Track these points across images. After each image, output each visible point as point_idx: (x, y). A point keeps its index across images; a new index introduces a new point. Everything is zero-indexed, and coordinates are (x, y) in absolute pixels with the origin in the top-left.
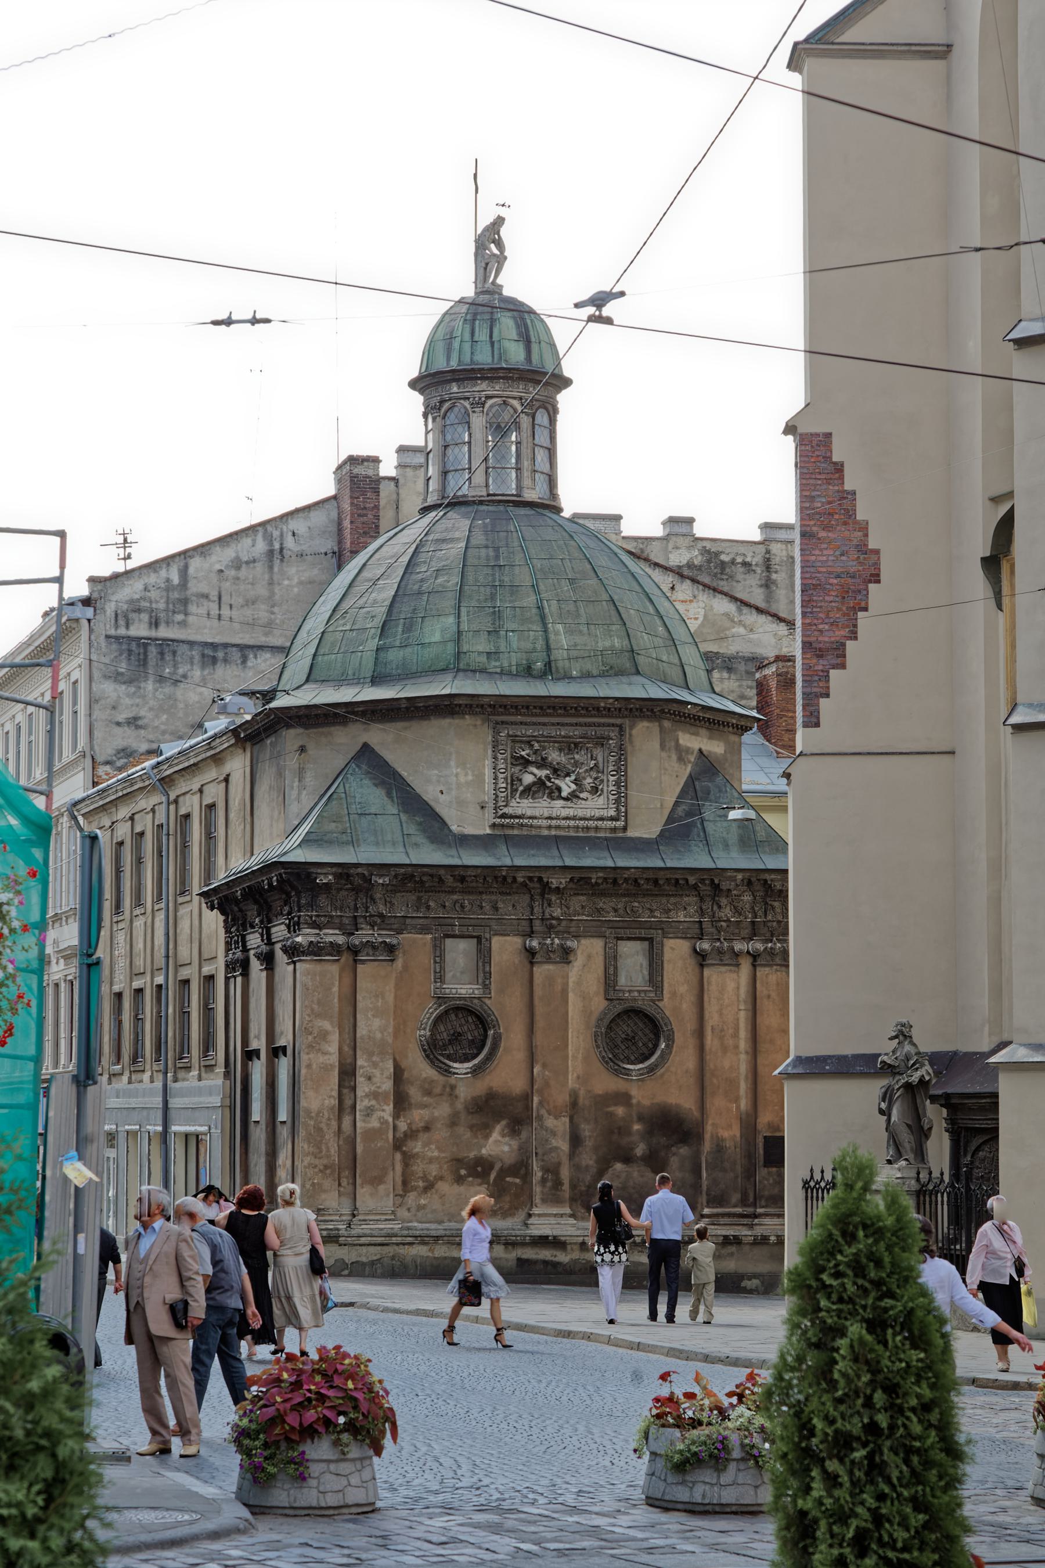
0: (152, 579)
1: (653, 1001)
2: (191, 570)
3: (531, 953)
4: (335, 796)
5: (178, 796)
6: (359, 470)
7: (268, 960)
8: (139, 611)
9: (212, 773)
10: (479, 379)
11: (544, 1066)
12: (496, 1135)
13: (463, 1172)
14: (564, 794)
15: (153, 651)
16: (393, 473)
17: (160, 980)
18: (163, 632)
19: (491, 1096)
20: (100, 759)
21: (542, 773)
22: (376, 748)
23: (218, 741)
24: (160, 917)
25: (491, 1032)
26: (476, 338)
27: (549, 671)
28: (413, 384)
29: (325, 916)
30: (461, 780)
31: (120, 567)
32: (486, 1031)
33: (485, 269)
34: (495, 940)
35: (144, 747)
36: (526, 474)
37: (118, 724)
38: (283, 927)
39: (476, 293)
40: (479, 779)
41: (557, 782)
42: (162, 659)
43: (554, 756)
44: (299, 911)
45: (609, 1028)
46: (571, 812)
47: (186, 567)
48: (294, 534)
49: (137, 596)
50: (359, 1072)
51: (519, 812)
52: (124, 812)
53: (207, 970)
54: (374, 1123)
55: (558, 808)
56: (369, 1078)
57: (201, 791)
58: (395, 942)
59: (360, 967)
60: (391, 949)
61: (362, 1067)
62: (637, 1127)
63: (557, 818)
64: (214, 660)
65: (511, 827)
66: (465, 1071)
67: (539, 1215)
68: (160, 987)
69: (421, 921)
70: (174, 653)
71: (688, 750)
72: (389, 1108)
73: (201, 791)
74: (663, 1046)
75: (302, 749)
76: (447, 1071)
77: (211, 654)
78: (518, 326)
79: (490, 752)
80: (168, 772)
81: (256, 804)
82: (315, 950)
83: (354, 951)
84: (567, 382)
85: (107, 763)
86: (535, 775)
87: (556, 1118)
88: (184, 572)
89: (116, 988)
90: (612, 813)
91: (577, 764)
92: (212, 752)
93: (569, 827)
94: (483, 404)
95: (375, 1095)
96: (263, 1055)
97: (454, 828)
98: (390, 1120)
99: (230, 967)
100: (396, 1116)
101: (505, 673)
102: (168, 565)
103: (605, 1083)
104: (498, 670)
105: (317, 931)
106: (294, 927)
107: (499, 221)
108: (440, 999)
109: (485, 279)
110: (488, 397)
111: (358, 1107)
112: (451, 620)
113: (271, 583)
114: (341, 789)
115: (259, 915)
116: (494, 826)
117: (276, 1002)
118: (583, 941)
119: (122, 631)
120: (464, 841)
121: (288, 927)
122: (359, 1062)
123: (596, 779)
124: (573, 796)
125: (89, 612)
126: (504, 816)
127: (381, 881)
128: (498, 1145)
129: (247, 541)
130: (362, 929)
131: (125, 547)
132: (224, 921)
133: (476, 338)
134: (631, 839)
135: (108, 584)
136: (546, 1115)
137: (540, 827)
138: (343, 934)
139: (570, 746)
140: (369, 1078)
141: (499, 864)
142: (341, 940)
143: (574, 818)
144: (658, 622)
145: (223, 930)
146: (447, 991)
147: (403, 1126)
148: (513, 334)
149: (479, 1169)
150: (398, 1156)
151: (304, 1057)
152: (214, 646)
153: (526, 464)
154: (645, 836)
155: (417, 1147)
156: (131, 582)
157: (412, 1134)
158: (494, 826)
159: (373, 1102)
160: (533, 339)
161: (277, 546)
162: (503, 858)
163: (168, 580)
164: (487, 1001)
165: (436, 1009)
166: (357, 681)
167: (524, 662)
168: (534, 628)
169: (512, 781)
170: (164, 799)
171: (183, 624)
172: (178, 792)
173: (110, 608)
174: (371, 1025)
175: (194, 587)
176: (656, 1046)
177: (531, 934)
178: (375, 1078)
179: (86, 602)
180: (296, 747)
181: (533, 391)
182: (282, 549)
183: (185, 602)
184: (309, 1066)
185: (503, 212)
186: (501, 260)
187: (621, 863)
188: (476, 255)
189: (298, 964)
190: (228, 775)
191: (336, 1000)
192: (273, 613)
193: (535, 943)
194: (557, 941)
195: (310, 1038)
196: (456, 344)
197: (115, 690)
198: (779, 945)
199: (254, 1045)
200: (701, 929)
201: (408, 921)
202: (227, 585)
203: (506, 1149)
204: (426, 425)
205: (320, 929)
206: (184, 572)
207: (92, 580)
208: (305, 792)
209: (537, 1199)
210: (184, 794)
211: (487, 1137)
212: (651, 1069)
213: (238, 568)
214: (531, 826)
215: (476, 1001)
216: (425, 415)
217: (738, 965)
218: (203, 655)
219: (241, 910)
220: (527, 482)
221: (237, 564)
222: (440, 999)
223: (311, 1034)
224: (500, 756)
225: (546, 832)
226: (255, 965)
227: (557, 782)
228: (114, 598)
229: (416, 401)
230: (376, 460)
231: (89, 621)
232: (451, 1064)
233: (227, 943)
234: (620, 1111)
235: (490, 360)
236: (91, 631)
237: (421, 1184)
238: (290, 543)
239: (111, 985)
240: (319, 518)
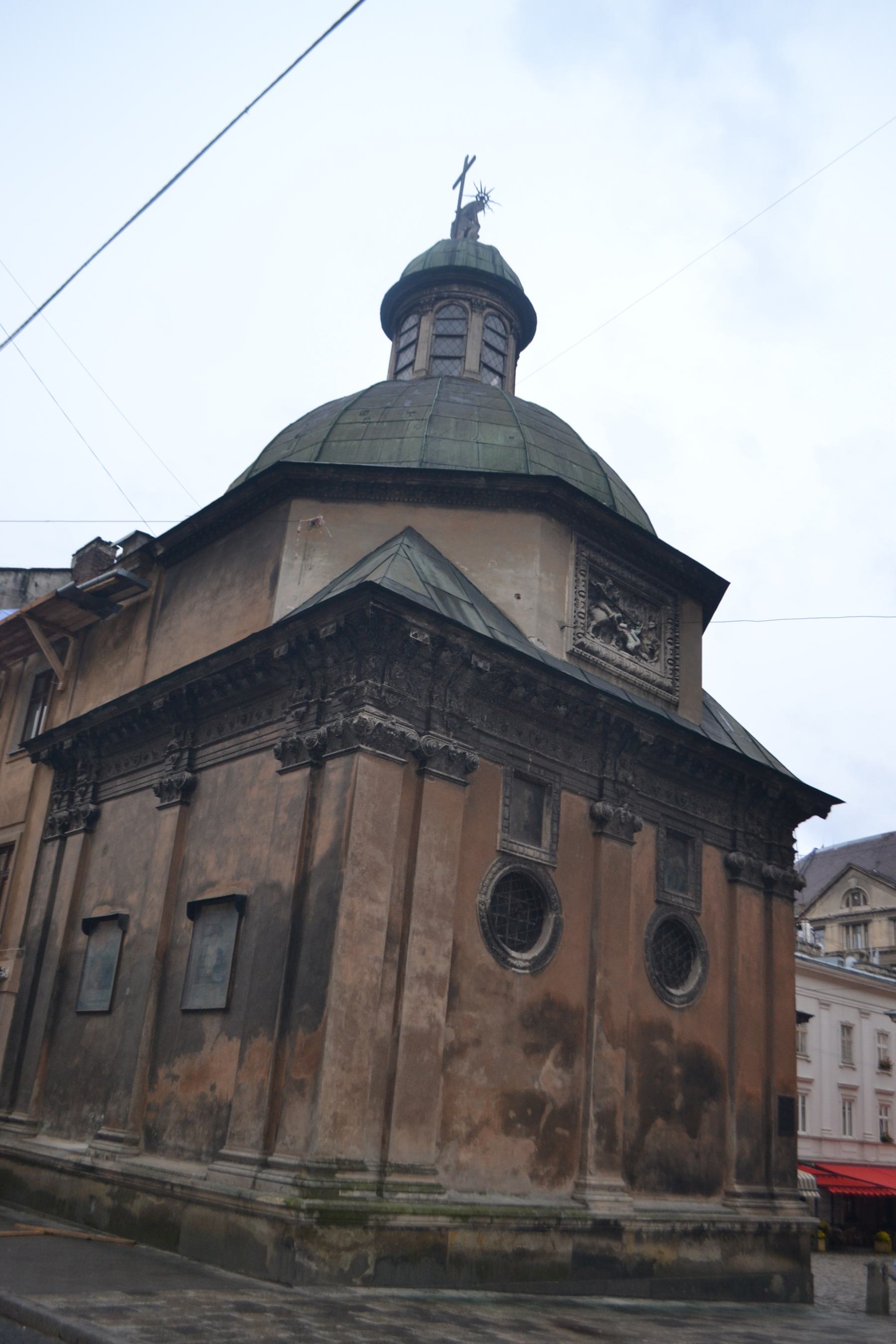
1: (692, 913)
3: (599, 821)
11: (606, 974)
12: (549, 1064)
13: (512, 1114)
19: (549, 1003)
29: (398, 695)
40: (561, 592)
44: (358, 680)
45: (657, 937)
54: (424, 1024)
59: (428, 783)
61: (417, 933)
62: (677, 1070)
63: (625, 669)
66: (522, 964)
67: (595, 1188)
69: (495, 744)
72: (442, 1003)
74: (700, 971)
76: (503, 961)
79: (571, 568)
86: (607, 613)
87: (614, 1048)
90: (668, 683)
94: (483, 308)
97: (533, 640)
98: (442, 1020)
100: (447, 1017)
103: (653, 1008)
108: (506, 856)
115: (177, 735)
116: (571, 654)
122: (414, 925)
126: (581, 646)
127: (481, 665)
128: (549, 1078)
130: (435, 729)
136: (604, 1041)
137: (610, 673)
139: (635, 598)
140: (423, 952)
143: (638, 675)
146: (515, 847)
149: (523, 1111)
151: (345, 902)
155: (462, 1067)
158: (571, 654)
159: (425, 991)
164: (550, 871)
165: (500, 869)
174: (434, 872)
177: (600, 797)
184: (350, 916)
191: (395, 822)
195: (357, 870)
201: (482, 738)
203: (559, 1084)
208: (309, 574)
209: (591, 1165)
211: (542, 1063)
212: (690, 997)
215: (540, 870)
222: (506, 856)
223: (358, 864)
224: (581, 578)
232: (509, 950)
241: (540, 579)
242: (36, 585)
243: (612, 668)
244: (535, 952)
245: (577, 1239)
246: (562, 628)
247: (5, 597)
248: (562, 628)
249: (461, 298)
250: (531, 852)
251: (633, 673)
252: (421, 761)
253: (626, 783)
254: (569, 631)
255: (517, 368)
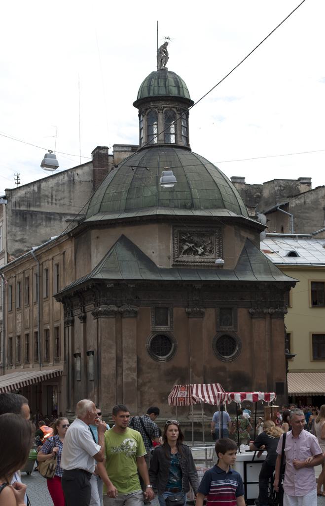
0: (28, 189)
2: (42, 187)
4: (112, 254)
5: (43, 262)
6: (101, 151)
7: (84, 319)
8: (23, 201)
9: (57, 252)
10: (161, 100)
14: (199, 253)
15: (28, 216)
16: (112, 154)
17: (37, 330)
18: (32, 209)
20: (10, 253)
21: (192, 245)
22: (127, 236)
23: (61, 238)
24: (37, 306)
25: (173, 344)
26: (159, 85)
27: (192, 207)
28: (136, 104)
30: (159, 249)
31: (16, 186)
32: (171, 344)
33: (161, 61)
34: (174, 309)
35: (26, 249)
36: (179, 136)
37: (16, 241)
38: (93, 305)
39: (158, 70)
40: (168, 247)
41: (197, 248)
42: (32, 218)
43: (196, 239)
44: (100, 298)
46: (202, 260)
47: (40, 186)
48: (78, 174)
49: (22, 196)
50: (124, 360)
51: (183, 260)
52: (20, 271)
53: (56, 325)
54: (130, 380)
55: (197, 258)
56: (128, 363)
57: (53, 259)
58: (136, 309)
60: (136, 313)
61: (125, 358)
62: (228, 380)
63: (197, 262)
64: (50, 219)
65: (180, 265)
66: (163, 359)
68: (36, 333)
70: (36, 216)
71: (243, 237)
72: (135, 374)
73: (53, 259)
74: (238, 349)
75: (98, 237)
76: (157, 360)
77: (49, 217)
78: (175, 82)
79: (171, 237)
80: (40, 253)
81: (77, 261)
82: (106, 313)
83: (121, 313)
84: (191, 103)
85: (12, 255)
86: (188, 246)
88: (39, 188)
89: (18, 334)
91: (204, 242)
92: (58, 243)
93: (201, 266)
94: (163, 110)
95: (130, 369)
96: (82, 356)
97: (158, 266)
98: (136, 378)
99: (66, 323)
100: (138, 377)
101: (176, 207)
102: (34, 185)
103: (216, 363)
104: (173, 206)
105: (107, 306)
106: (97, 304)
107: (166, 44)
108: (154, 332)
109: (161, 65)
110: (165, 107)
111: (124, 374)
112: (155, 187)
113: (70, 192)
114: (115, 251)
117: (88, 334)
118: (208, 309)
119: (18, 208)
120: (162, 271)
121: (94, 305)
122: (124, 357)
123: (211, 247)
124: (203, 254)
125: (6, 201)
126: (177, 261)
127: (132, 286)
129: (61, 177)
131: (18, 180)
132: (64, 306)
133: (159, 85)
134: (224, 270)
135: (12, 192)
137: (191, 266)
138: (117, 307)
139: (202, 235)
140: (128, 363)
141: (177, 279)
142: (116, 309)
143: (203, 262)
144: (230, 190)
145: (63, 310)
147: (141, 381)
148: (174, 84)
150: (139, 393)
151: (102, 354)
152: (50, 214)
153: (179, 132)
154: (230, 269)
155: (146, 389)
156: (21, 191)
157: (144, 384)
158: (173, 265)
159: (129, 372)
160: (180, 86)
161: (72, 179)
162: (178, 277)
163: (34, 190)
164: (172, 333)
166: (119, 211)
167: (183, 204)
168: (187, 190)
169: (180, 248)
170: (38, 263)
171: (39, 206)
172: (43, 261)
173: (13, 200)
174: (128, 342)
175: (42, 193)
176: (234, 349)
177: (188, 307)
178: (129, 362)
179: (5, 198)
180: (96, 237)
181: (181, 106)
182: (74, 180)
183: (40, 198)
184: (104, 358)
185: (167, 41)
186: (167, 58)
187: (222, 279)
188: (158, 56)
189: (99, 319)
190: (64, 252)
192: (71, 202)
193: (190, 310)
194: (198, 309)
196: (152, 88)
197: (15, 229)
198: (280, 310)
199: (77, 352)
200: (251, 304)
202: (54, 192)
204: (140, 119)
205: (108, 305)
206: (39, 188)
207: (6, 190)
210: (45, 261)
212: (233, 357)
213: (58, 186)
214: (187, 265)
216: (139, 116)
217: (265, 318)
218: (46, 217)
219: (71, 301)
220: (179, 139)
221: (58, 184)
222: (154, 332)
224: (175, 239)
225: (193, 268)
226: (77, 321)
227: (197, 248)
228: (14, 197)
229: (136, 111)
230: (107, 148)
231: (6, 204)
233: (65, 314)
234: (222, 374)
235: (165, 93)
236: (6, 208)
237: (148, 403)
238: (76, 178)
239: (16, 333)
240: (86, 169)
241: (159, 246)
242: (78, 174)
243: (191, 264)
244: (168, 356)
245: (186, 428)
246: (169, 258)
247: (65, 185)
248: (169, 258)
249: (154, 108)
250: (163, 328)
251: (200, 262)
252: (120, 315)
253: (196, 300)
254: (172, 257)
255: (189, 118)
